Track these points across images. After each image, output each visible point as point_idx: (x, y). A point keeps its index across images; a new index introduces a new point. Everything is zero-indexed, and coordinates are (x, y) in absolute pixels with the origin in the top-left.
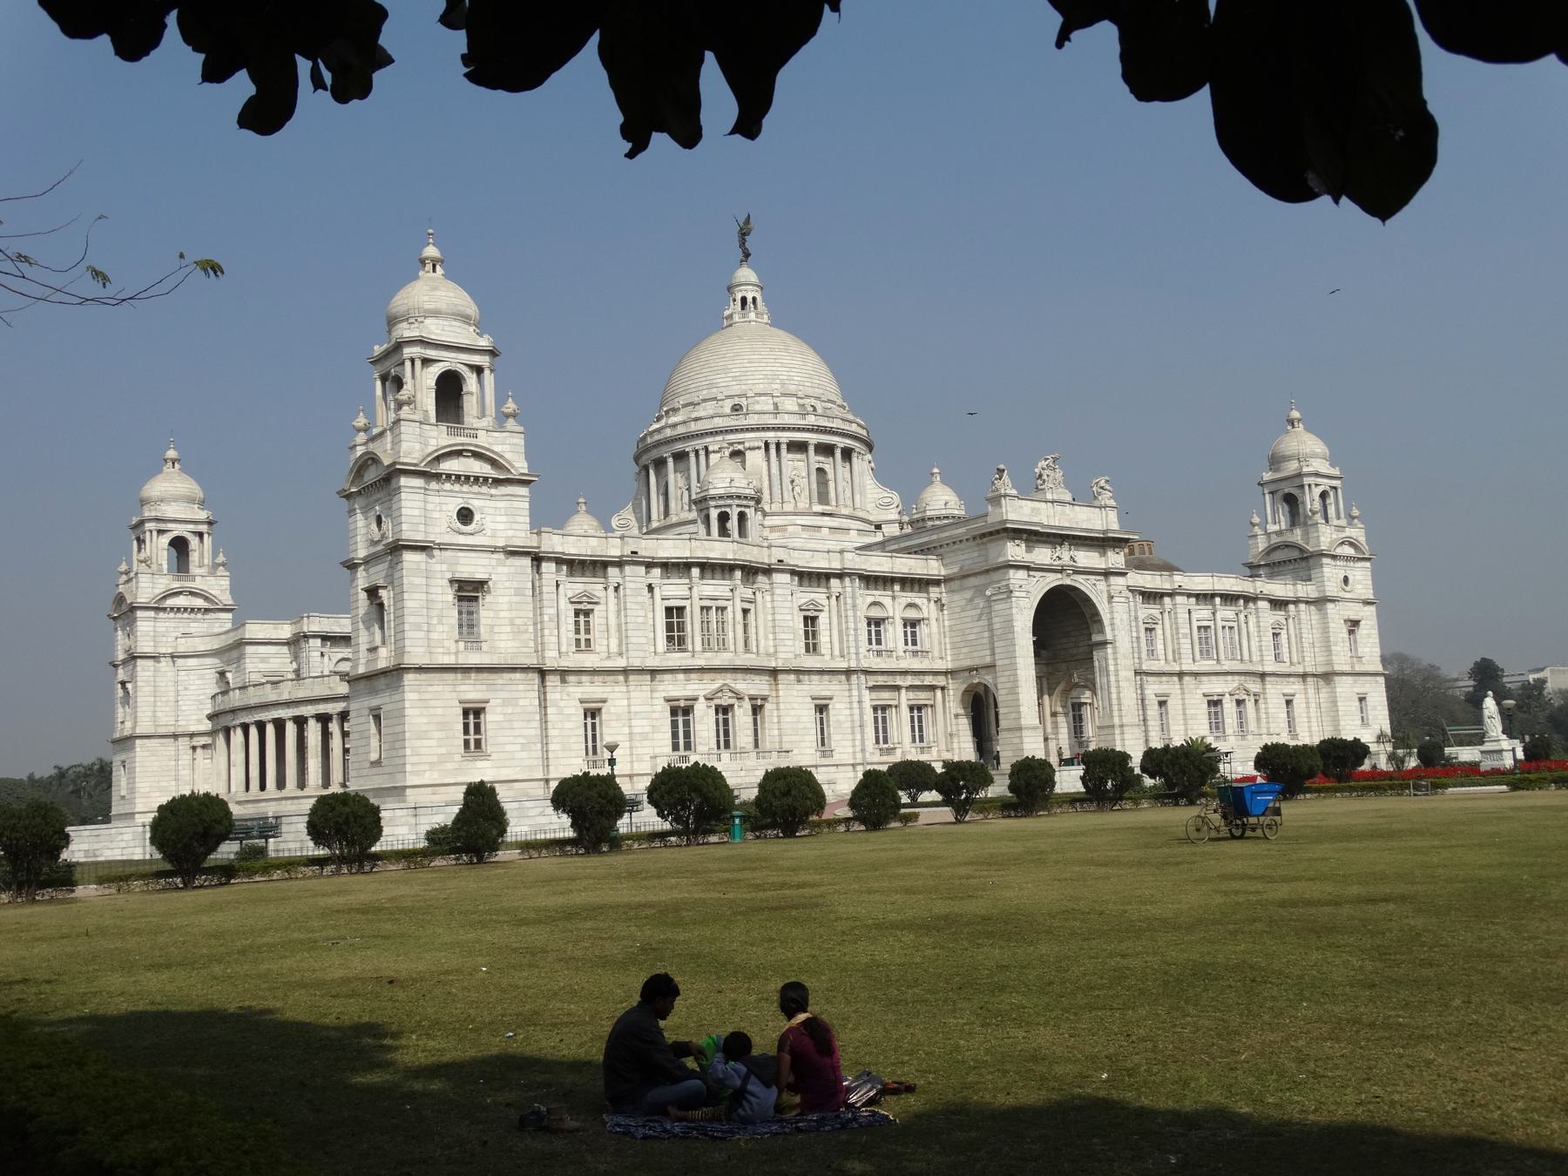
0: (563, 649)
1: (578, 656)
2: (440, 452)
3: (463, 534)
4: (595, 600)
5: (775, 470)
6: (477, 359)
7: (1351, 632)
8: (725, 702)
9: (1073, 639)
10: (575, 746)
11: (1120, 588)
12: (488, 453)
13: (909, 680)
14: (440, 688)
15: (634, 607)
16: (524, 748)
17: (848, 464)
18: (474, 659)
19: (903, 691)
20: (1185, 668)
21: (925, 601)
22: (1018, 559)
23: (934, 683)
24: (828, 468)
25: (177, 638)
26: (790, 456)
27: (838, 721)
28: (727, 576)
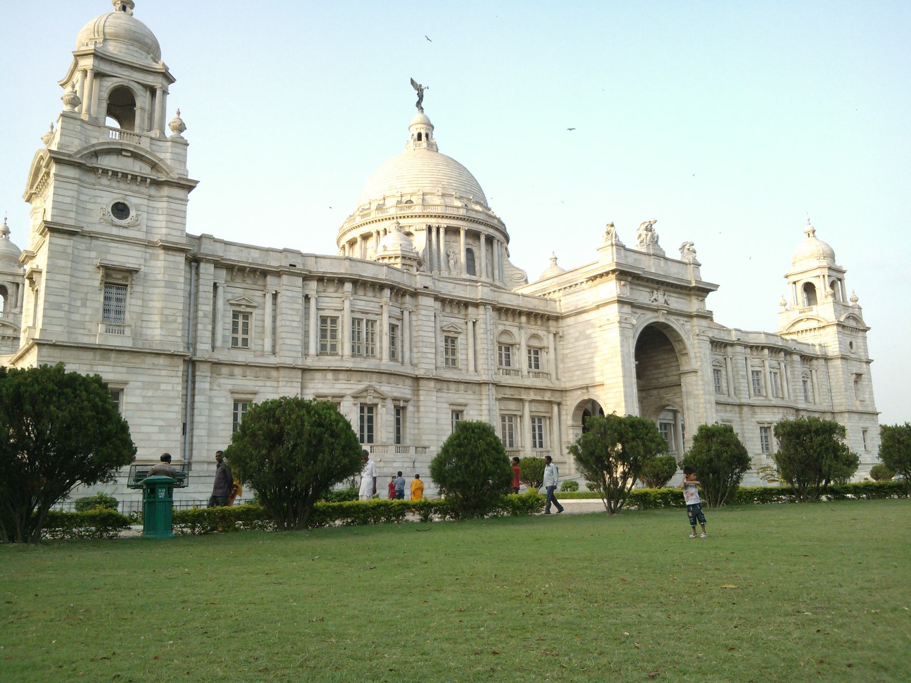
0: (219, 343)
1: (233, 352)
2: (97, 148)
3: (116, 226)
6: (150, 80)
7: (856, 382)
8: (369, 400)
9: (663, 370)
10: (223, 433)
11: (703, 329)
12: (147, 156)
13: (532, 396)
16: (162, 429)
17: (490, 247)
19: (527, 405)
20: (744, 401)
21: (545, 333)
22: (625, 296)
23: (552, 399)
24: (474, 249)
26: (448, 238)
28: (378, 295)
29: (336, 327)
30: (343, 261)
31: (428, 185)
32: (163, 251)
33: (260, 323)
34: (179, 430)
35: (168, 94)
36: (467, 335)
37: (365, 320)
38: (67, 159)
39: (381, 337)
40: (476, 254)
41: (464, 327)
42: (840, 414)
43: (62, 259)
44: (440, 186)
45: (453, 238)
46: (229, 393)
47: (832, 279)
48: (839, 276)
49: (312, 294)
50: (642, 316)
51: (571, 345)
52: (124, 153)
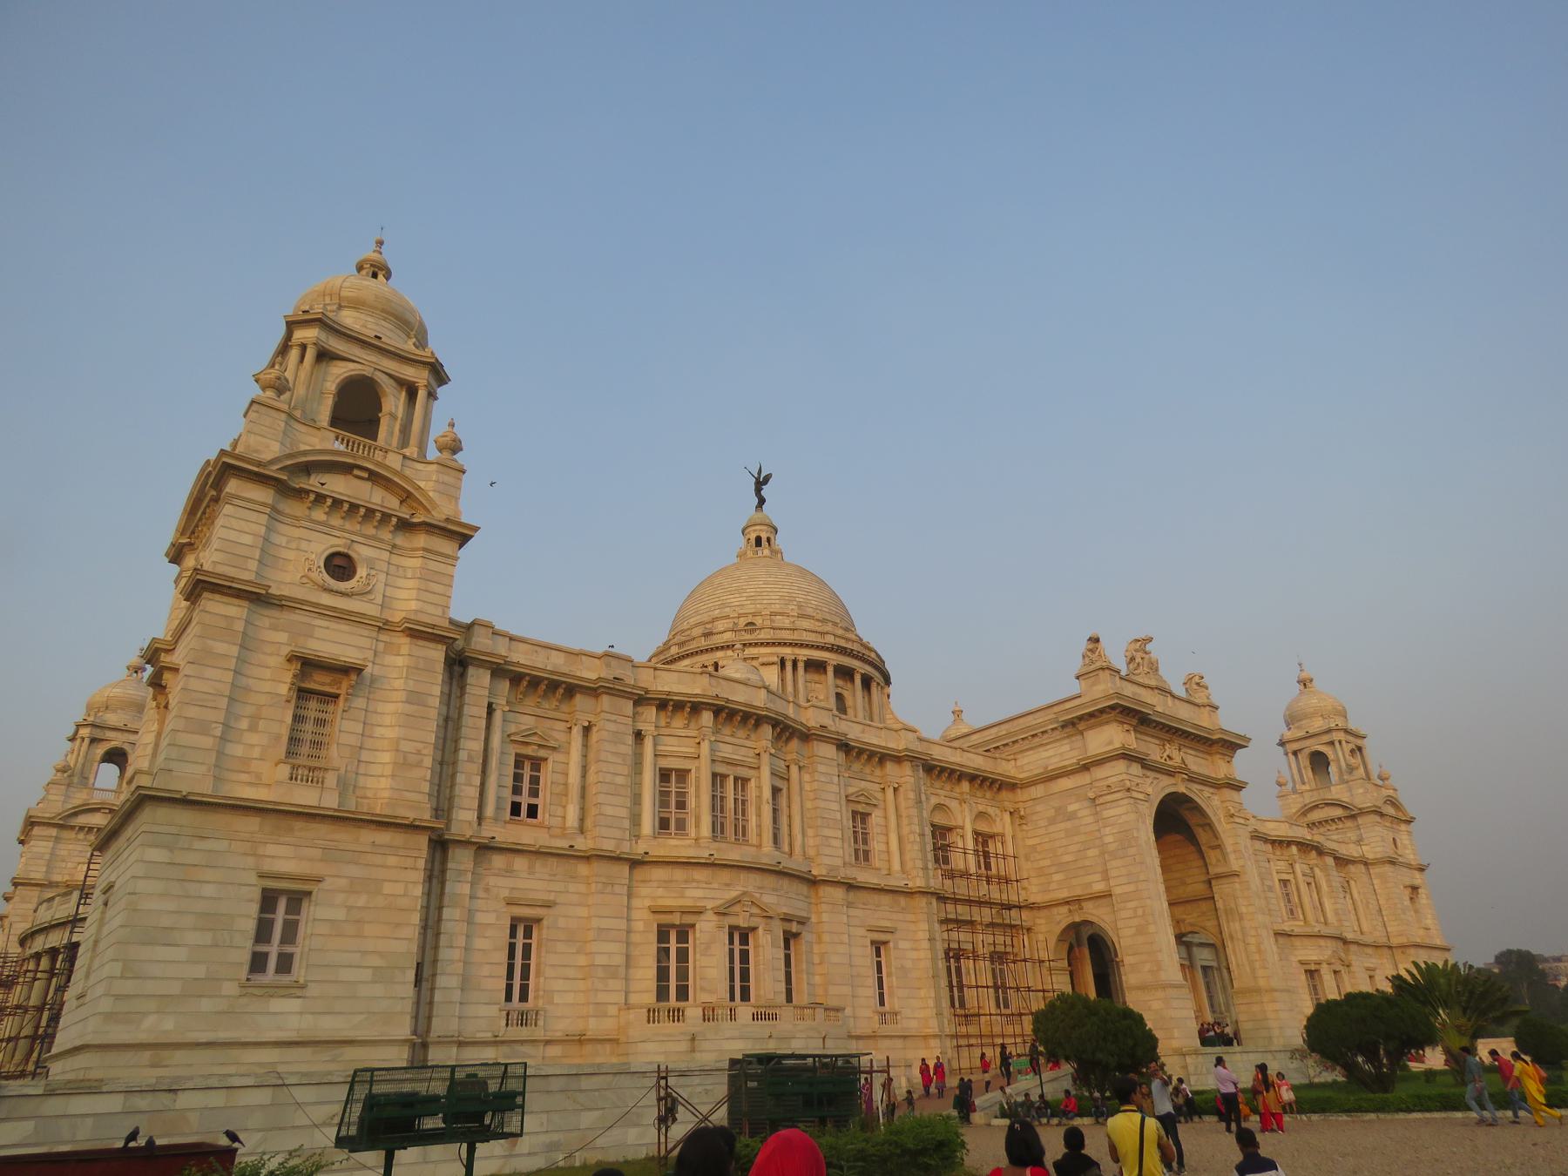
0: (490, 810)
3: (330, 591)
4: (552, 743)
5: (790, 688)
6: (409, 373)
8: (742, 922)
14: (221, 845)
15: (611, 758)
17: (866, 693)
18: (305, 797)
21: (998, 811)
24: (845, 693)
25: (79, 863)
26: (810, 676)
27: (902, 967)
28: (753, 736)
29: (684, 788)
30: (698, 676)
31: (777, 601)
32: (408, 640)
33: (559, 778)
34: (411, 975)
35: (436, 398)
36: (885, 809)
37: (732, 778)
38: (256, 469)
39: (759, 808)
40: (849, 702)
41: (879, 795)
42: (1400, 950)
43: (222, 641)
44: (795, 603)
45: (816, 677)
46: (504, 903)
47: (1351, 746)
48: (1359, 742)
49: (647, 728)
50: (1155, 782)
51: (1042, 831)
52: (356, 472)
